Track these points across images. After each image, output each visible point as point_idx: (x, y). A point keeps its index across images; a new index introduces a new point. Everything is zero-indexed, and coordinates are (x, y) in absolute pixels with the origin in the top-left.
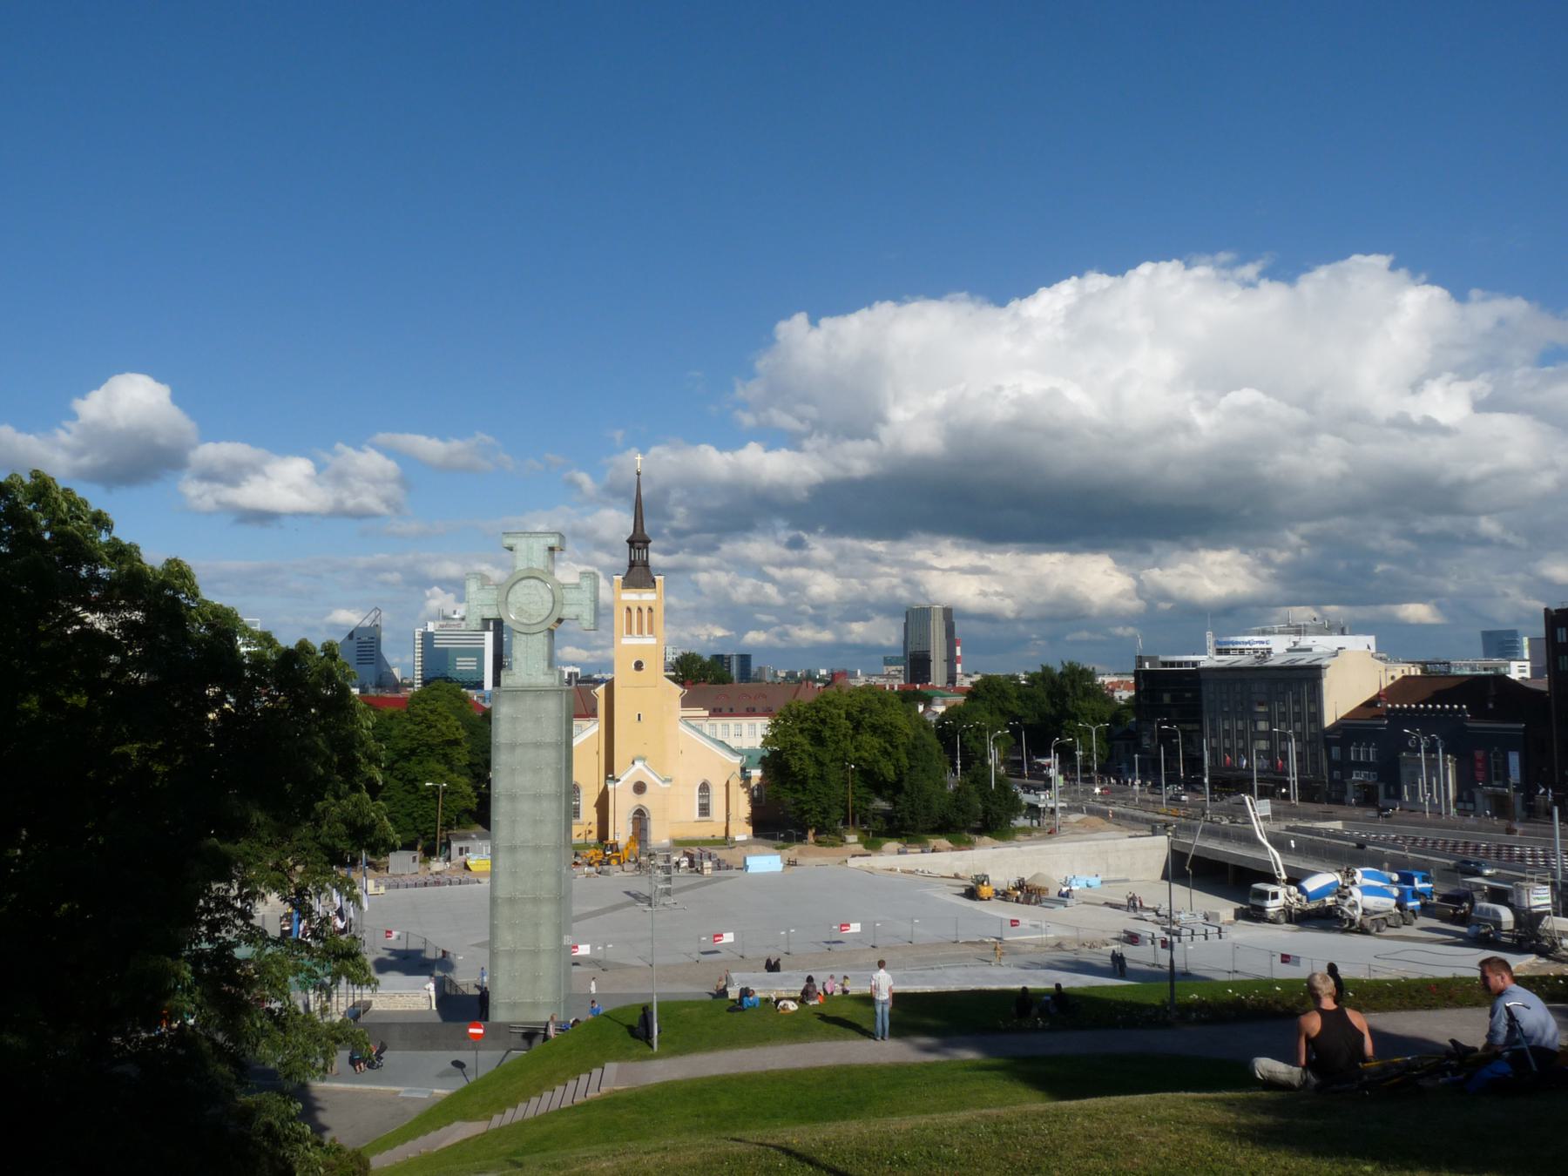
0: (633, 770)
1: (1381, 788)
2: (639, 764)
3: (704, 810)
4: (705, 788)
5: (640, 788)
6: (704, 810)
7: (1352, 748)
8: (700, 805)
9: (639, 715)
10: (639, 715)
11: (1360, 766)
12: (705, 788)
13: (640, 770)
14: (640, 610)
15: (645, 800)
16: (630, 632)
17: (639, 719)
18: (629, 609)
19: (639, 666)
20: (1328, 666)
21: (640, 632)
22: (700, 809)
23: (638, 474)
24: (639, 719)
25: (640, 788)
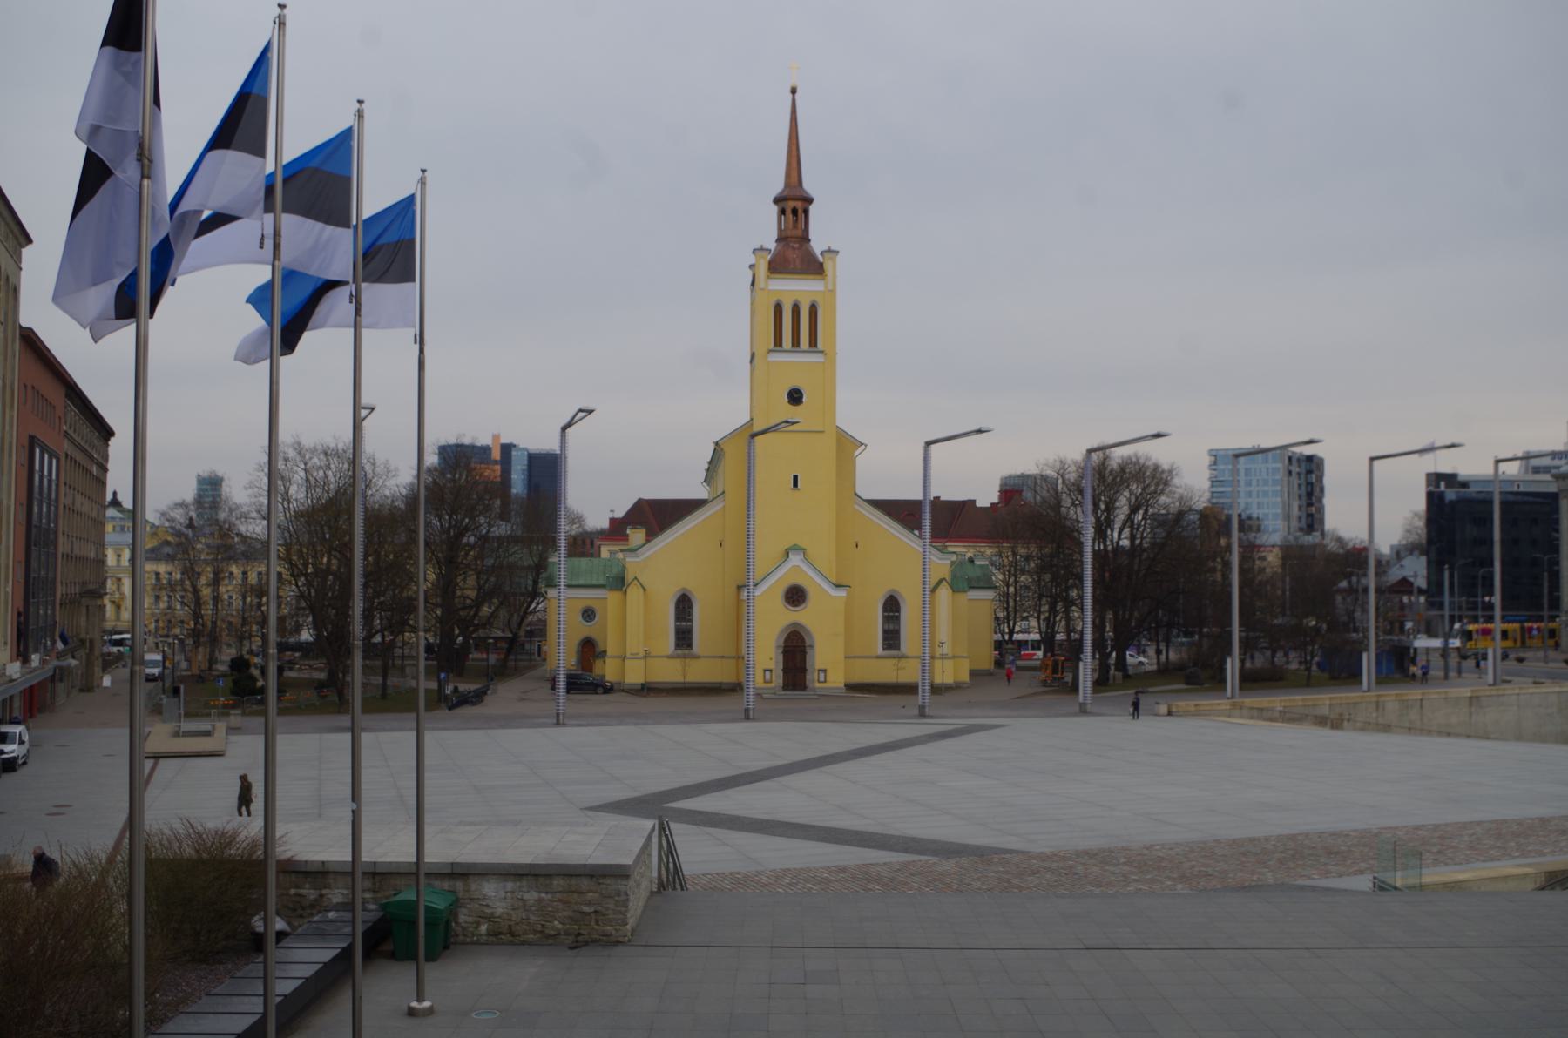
2: (795, 559)
4: (892, 606)
5: (795, 596)
9: (795, 478)
10: (795, 478)
14: (796, 309)
15: (802, 616)
16: (778, 341)
17: (795, 484)
18: (778, 309)
19: (795, 397)
21: (796, 342)
22: (885, 639)
23: (794, 91)
24: (795, 484)
25: (795, 596)
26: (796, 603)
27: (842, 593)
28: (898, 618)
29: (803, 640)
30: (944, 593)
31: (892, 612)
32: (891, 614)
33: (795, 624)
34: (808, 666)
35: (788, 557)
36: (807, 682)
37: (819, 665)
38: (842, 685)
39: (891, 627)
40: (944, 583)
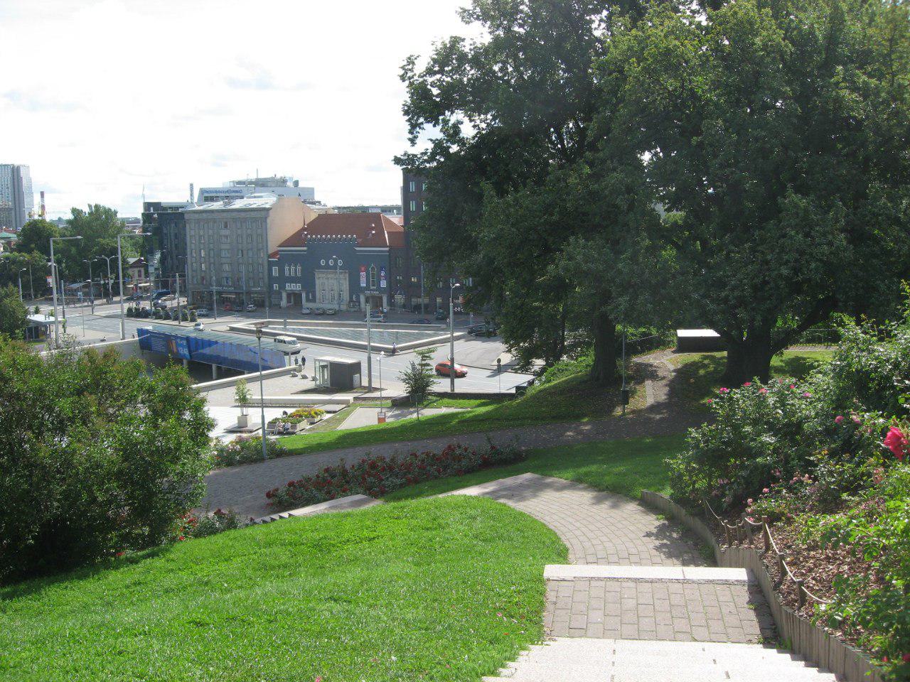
1: (304, 295)
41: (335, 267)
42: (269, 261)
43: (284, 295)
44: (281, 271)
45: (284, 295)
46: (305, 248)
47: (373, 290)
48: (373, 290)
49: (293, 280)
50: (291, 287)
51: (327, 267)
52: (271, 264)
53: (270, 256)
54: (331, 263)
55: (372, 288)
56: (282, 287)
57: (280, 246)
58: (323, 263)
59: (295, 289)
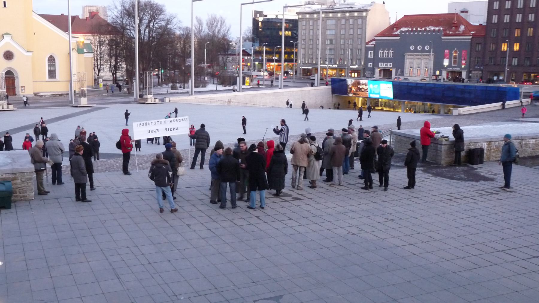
0: (4, 42)
2: (7, 39)
3: (52, 74)
4: (52, 59)
6: (52, 74)
7: (380, 51)
8: (49, 71)
9: (5, 3)
10: (5, 3)
11: (384, 60)
12: (52, 59)
13: (7, 43)
15: (11, 64)
17: (5, 6)
20: (370, 10)
22: (49, 74)
24: (5, 6)
26: (9, 58)
27: (29, 54)
28: (55, 65)
29: (13, 74)
30: (74, 54)
31: (52, 62)
32: (51, 63)
33: (9, 67)
34: (16, 86)
35: (4, 38)
36: (16, 92)
37: (21, 85)
38: (33, 93)
39: (52, 69)
40: (74, 50)
41: (423, 50)
42: (366, 47)
43: (377, 71)
44: (376, 54)
45: (377, 71)
46: (399, 38)
47: (455, 67)
48: (455, 67)
49: (387, 60)
50: (383, 65)
51: (416, 50)
52: (367, 49)
53: (367, 44)
54: (419, 48)
55: (453, 65)
56: (376, 65)
57: (376, 37)
58: (412, 48)
59: (387, 66)
